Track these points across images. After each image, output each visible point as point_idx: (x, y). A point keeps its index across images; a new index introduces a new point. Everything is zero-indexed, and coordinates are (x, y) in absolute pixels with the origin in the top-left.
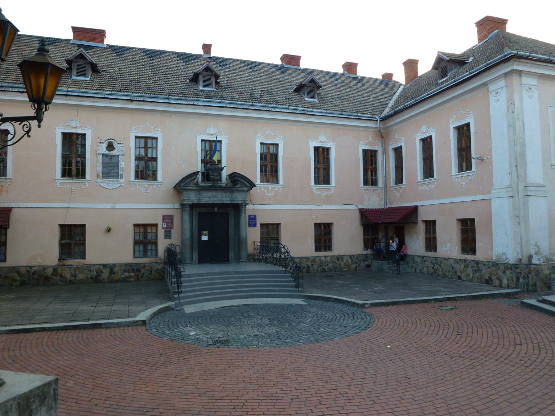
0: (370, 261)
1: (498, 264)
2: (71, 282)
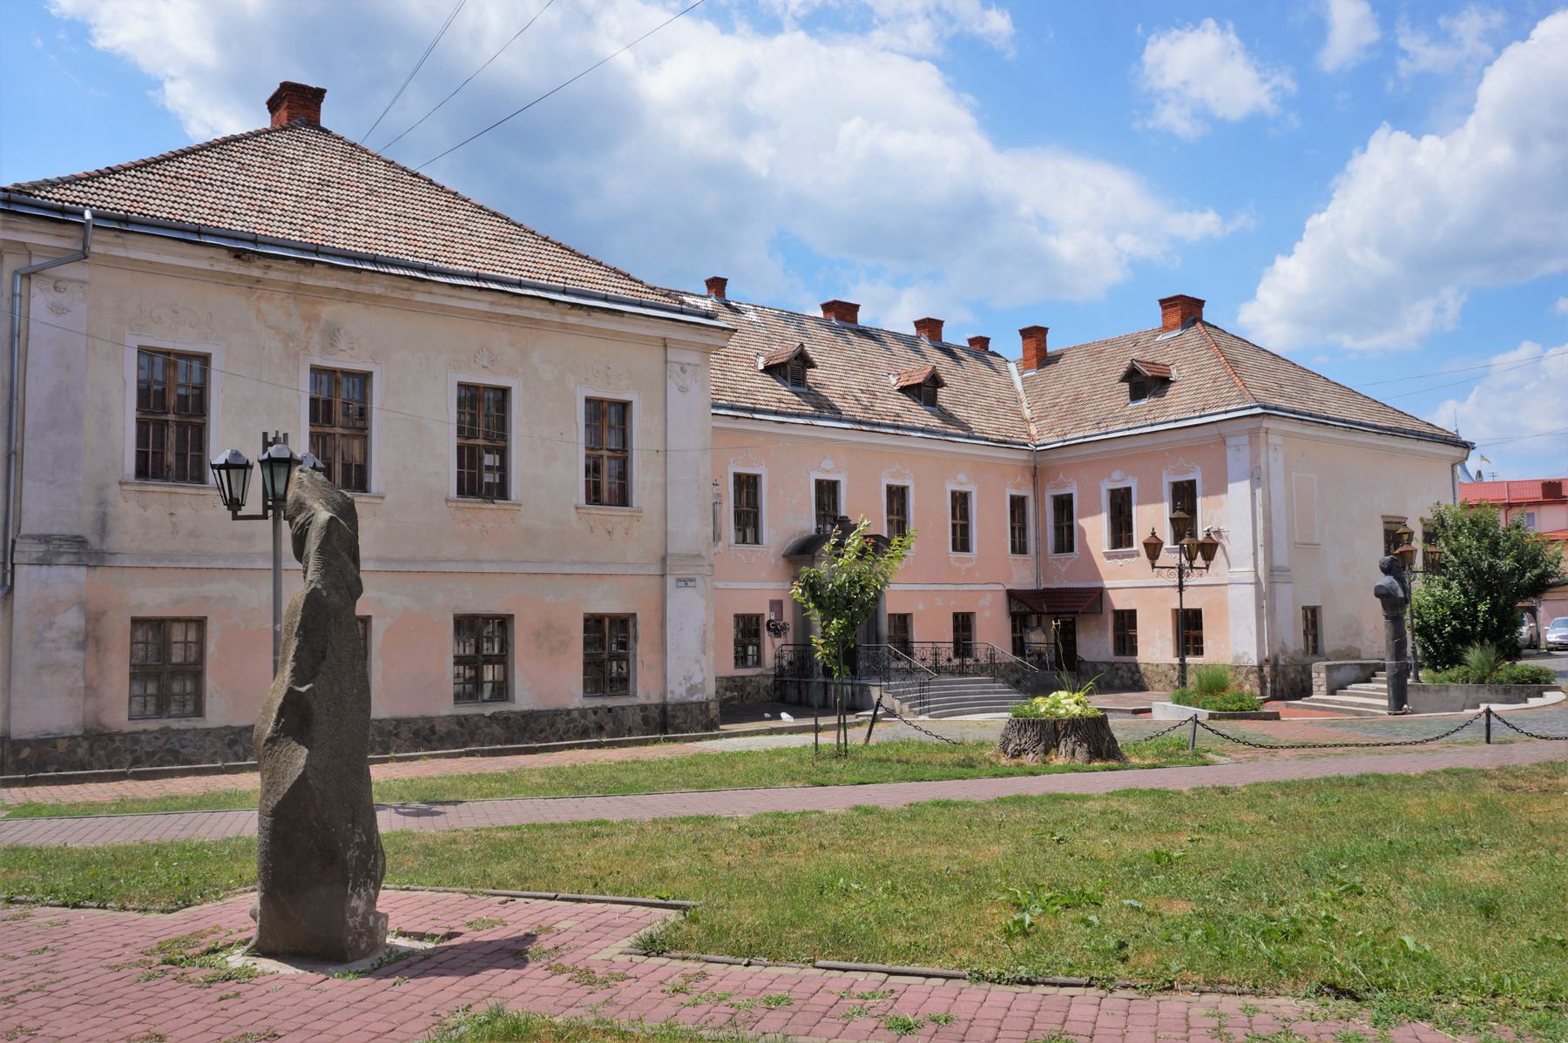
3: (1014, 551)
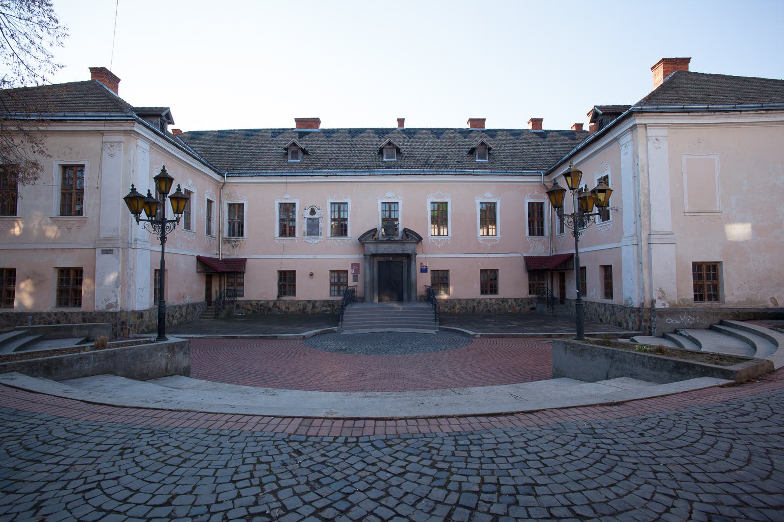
0: (535, 304)
1: (625, 308)
2: (285, 312)
3: (530, 234)
